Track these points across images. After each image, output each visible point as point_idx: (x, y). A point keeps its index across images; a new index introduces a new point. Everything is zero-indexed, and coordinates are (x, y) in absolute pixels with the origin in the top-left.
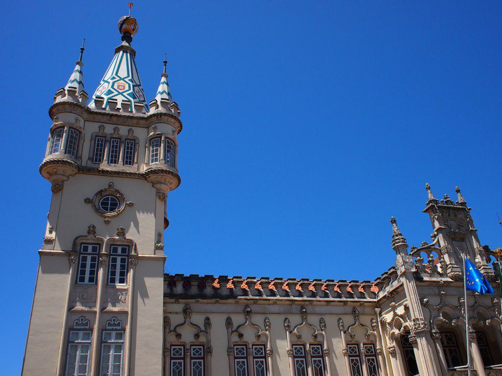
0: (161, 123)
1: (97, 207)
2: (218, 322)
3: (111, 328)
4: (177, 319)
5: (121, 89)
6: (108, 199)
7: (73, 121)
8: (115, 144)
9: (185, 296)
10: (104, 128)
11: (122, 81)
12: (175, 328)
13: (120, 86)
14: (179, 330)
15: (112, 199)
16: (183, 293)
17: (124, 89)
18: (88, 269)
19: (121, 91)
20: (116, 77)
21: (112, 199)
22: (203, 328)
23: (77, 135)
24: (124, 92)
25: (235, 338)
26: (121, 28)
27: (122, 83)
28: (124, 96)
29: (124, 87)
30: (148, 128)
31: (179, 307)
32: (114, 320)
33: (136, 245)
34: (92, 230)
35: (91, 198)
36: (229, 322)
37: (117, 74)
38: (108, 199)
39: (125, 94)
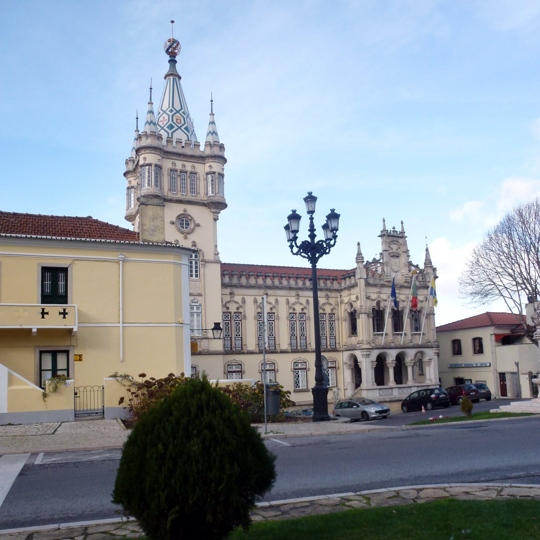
0: (215, 162)
5: (179, 123)
6: (183, 220)
7: (159, 163)
8: (183, 177)
12: (226, 304)
14: (228, 305)
16: (229, 282)
17: (181, 123)
19: (179, 125)
20: (173, 109)
21: (186, 221)
27: (178, 117)
28: (182, 130)
31: (228, 291)
33: (203, 254)
36: (255, 301)
39: (183, 128)
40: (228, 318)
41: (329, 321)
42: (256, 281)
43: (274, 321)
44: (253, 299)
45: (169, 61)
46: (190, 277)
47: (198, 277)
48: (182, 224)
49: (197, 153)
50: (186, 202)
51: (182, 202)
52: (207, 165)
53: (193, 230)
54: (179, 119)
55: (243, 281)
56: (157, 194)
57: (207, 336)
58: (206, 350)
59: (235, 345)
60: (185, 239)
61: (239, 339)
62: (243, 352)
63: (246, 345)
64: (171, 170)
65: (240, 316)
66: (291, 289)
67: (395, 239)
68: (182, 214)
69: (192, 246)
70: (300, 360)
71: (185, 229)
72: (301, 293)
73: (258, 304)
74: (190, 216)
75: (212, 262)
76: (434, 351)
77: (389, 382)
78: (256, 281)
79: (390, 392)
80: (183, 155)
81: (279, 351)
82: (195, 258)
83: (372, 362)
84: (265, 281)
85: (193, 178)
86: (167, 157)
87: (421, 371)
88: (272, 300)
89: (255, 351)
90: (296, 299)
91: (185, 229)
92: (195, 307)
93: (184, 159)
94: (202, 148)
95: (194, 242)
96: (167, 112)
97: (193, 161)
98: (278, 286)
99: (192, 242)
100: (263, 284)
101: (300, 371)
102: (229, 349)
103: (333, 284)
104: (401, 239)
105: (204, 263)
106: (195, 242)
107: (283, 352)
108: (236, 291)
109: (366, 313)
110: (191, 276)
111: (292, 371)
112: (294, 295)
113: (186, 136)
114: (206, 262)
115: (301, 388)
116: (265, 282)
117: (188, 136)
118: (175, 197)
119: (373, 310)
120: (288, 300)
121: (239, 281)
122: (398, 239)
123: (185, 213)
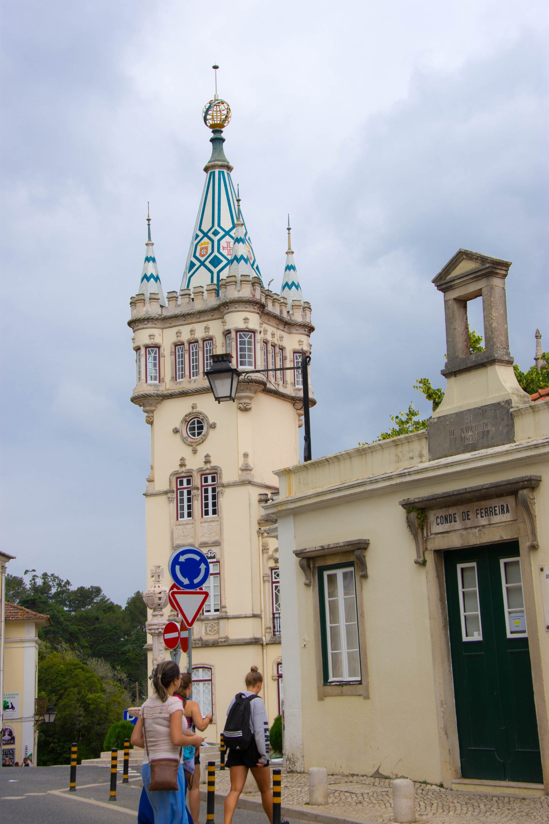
5: (203, 256)
7: (148, 342)
10: (181, 333)
11: (205, 239)
13: (203, 248)
15: (199, 422)
17: (207, 252)
19: (202, 259)
21: (199, 422)
23: (155, 354)
27: (205, 242)
28: (206, 267)
29: (206, 248)
32: (211, 553)
35: (178, 427)
37: (200, 230)
38: (193, 423)
45: (212, 140)
47: (216, 514)
50: (194, 392)
51: (188, 394)
53: (206, 436)
54: (205, 247)
57: (223, 614)
64: (176, 345)
68: (190, 414)
69: (206, 463)
71: (196, 437)
74: (201, 414)
80: (188, 314)
82: (212, 481)
85: (208, 348)
91: (198, 436)
93: (193, 321)
95: (207, 456)
97: (206, 319)
99: (206, 457)
105: (222, 489)
106: (210, 456)
110: (207, 513)
113: (210, 274)
114: (223, 486)
123: (195, 411)
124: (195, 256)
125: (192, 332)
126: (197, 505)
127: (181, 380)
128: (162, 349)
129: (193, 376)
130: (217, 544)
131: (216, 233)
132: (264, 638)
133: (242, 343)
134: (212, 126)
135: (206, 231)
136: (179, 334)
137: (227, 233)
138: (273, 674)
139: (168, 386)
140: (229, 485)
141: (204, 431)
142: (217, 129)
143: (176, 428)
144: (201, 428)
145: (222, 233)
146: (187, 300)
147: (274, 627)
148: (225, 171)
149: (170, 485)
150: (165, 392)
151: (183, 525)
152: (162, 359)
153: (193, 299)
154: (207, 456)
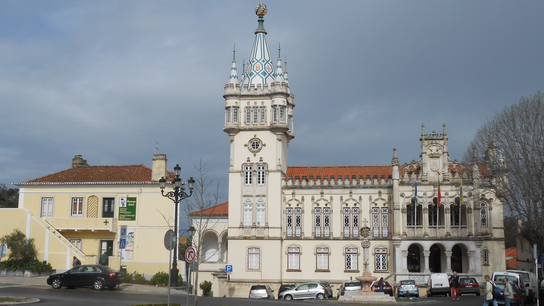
1: (250, 148)
2: (308, 198)
3: (260, 203)
4: (289, 197)
5: (257, 70)
7: (235, 105)
9: (293, 187)
13: (257, 67)
14: (290, 203)
16: (292, 185)
18: (249, 178)
19: (258, 72)
20: (254, 59)
22: (301, 201)
24: (259, 72)
25: (316, 206)
26: (257, 14)
29: (259, 67)
30: (271, 99)
31: (291, 191)
32: (261, 200)
34: (249, 161)
35: (247, 144)
37: (255, 58)
39: (260, 74)
40: (291, 212)
41: (382, 214)
42: (315, 183)
43: (329, 214)
44: (311, 197)
45: (259, 21)
46: (258, 183)
48: (253, 145)
49: (266, 91)
52: (272, 99)
53: (260, 149)
55: (304, 183)
56: (233, 127)
57: (267, 226)
58: (266, 236)
59: (295, 232)
60: (254, 156)
61: (299, 228)
62: (301, 238)
63: (303, 233)
64: (247, 108)
65: (300, 210)
66: (345, 188)
67: (434, 141)
68: (253, 139)
70: (351, 246)
71: (255, 149)
72: (354, 191)
73: (315, 201)
74: (259, 139)
75: (274, 171)
76: (476, 244)
77: (424, 269)
78: (315, 183)
79: (422, 278)
80: (254, 95)
81: (331, 238)
83: (402, 251)
84: (323, 183)
86: (244, 99)
87: (487, 262)
88: (327, 197)
89: (311, 238)
90: (350, 196)
92: (261, 205)
94: (270, 88)
95: (261, 158)
96: (252, 62)
98: (333, 186)
100: (320, 185)
101: (351, 255)
102: (290, 235)
103: (387, 183)
104: (442, 141)
107: (334, 239)
108: (297, 191)
109: (399, 209)
110: (259, 182)
111: (343, 255)
112: (348, 193)
115: (352, 269)
116: (322, 183)
117: (263, 79)
118: (248, 127)
119: (408, 206)
120: (341, 197)
121: (300, 183)
122: (438, 141)
124: (253, 70)
125: (255, 103)
126: (255, 179)
127: (248, 123)
128: (240, 108)
129: (255, 122)
130: (264, 196)
131: (263, 61)
132: (283, 238)
133: (281, 111)
134: (259, 15)
135: (258, 60)
136: (248, 103)
137: (268, 62)
138: (286, 252)
139: (243, 125)
140: (272, 171)
141: (260, 147)
142: (261, 15)
143: (246, 144)
144: (258, 145)
145: (266, 62)
146: (252, 89)
147: (287, 233)
148: (265, 34)
149: (242, 169)
150: (241, 128)
151: (248, 186)
152: (240, 113)
153: (256, 89)
154: (261, 158)
